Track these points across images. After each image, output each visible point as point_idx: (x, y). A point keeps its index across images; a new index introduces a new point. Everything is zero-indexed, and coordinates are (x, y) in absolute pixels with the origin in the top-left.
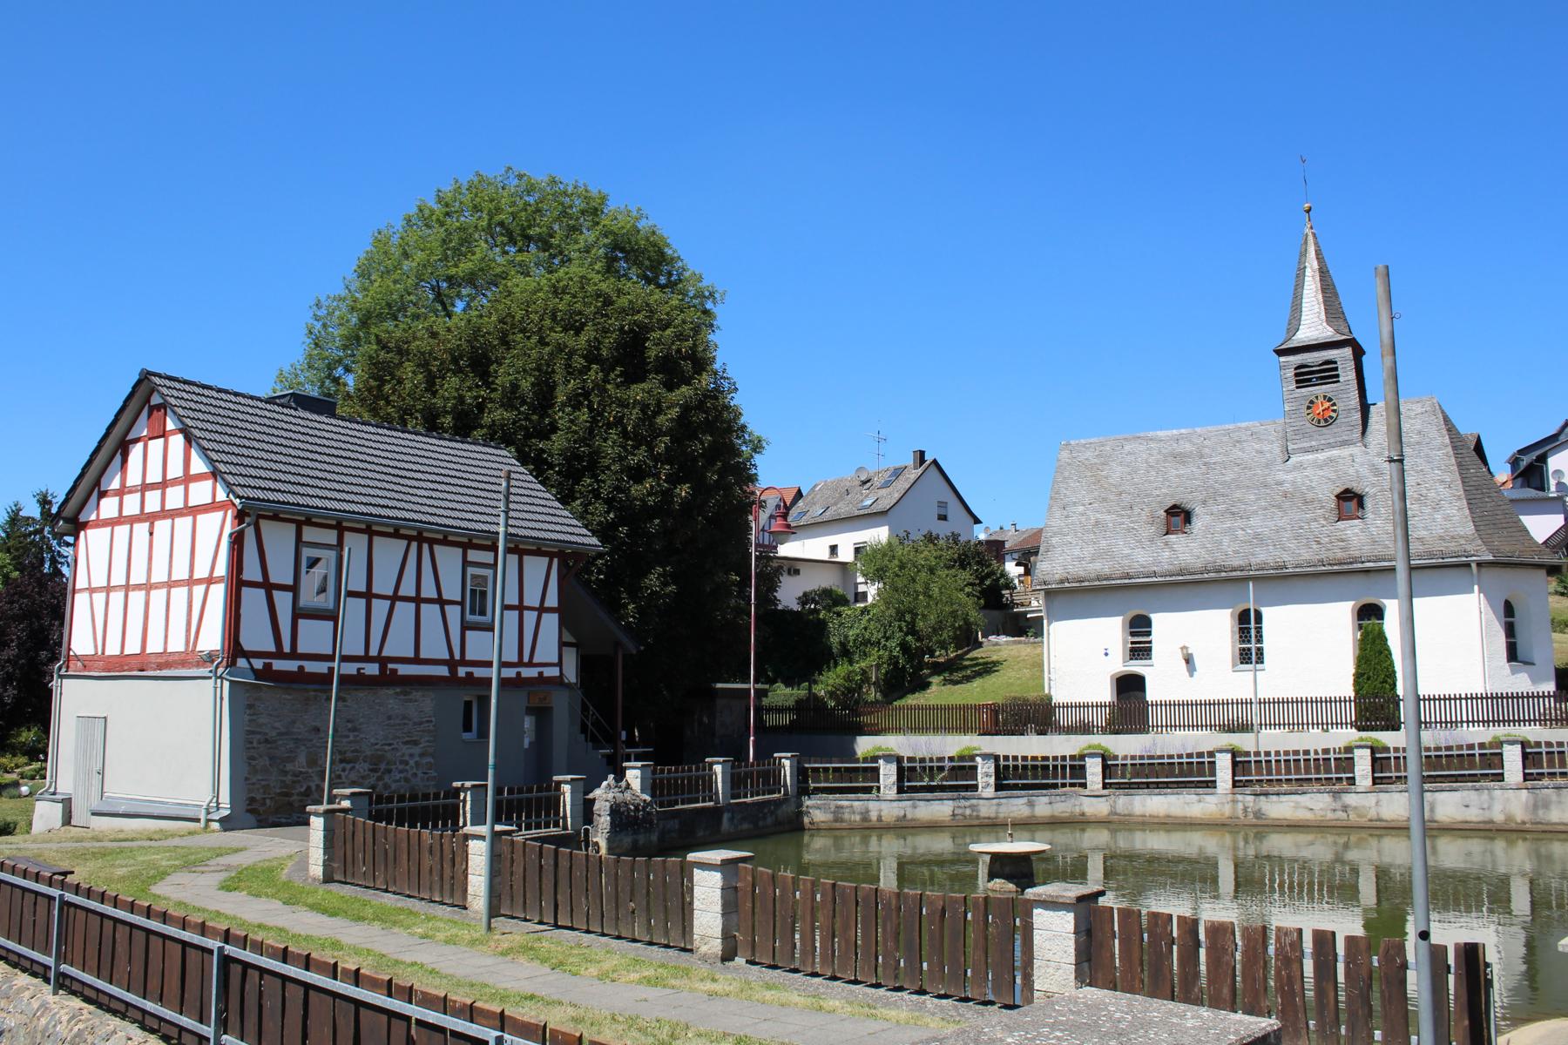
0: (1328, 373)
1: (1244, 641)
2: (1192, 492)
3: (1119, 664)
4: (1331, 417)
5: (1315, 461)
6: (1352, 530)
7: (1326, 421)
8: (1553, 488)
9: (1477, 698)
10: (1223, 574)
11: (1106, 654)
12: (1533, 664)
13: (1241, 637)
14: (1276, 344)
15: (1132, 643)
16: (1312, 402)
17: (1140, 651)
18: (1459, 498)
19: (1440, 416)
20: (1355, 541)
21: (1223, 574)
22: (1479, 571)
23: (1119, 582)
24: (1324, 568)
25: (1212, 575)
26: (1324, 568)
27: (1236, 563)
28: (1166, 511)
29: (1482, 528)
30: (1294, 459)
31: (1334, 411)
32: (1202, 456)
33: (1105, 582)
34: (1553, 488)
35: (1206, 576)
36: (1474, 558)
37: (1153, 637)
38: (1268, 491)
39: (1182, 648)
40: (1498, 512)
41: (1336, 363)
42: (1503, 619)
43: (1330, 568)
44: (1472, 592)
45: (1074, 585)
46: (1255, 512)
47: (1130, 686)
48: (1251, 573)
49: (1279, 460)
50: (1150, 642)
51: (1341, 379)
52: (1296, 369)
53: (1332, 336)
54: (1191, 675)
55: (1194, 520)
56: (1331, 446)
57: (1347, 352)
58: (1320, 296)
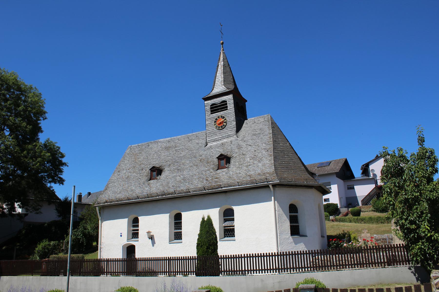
0: (223, 106)
1: (176, 229)
2: (167, 162)
3: (125, 241)
4: (224, 125)
5: (216, 145)
6: (222, 173)
7: (222, 127)
8: (372, 175)
9: (258, 256)
10: (164, 196)
11: (121, 236)
12: (306, 236)
13: (175, 227)
14: (203, 97)
15: (133, 230)
16: (216, 119)
17: (135, 235)
18: (271, 156)
19: (270, 122)
20: (222, 178)
21: (164, 196)
22: (274, 190)
23: (125, 202)
24: (205, 191)
25: (160, 197)
26: (205, 191)
27: (172, 190)
28: (150, 170)
29: (279, 169)
30: (209, 145)
31: (225, 122)
32: (176, 147)
33: (119, 202)
34: (372, 175)
35: (157, 197)
36: (271, 182)
37: (140, 228)
38: (195, 159)
39: (149, 232)
40: (291, 162)
41: (226, 101)
42: (289, 214)
43: (208, 191)
44: (271, 201)
45: (108, 204)
46: (187, 169)
47: (130, 250)
48: (175, 195)
49: (204, 146)
50: (138, 230)
51: (228, 108)
52: (211, 106)
53: (225, 90)
54: (153, 246)
55: (163, 173)
56: (223, 138)
57: (230, 97)
58: (223, 76)
